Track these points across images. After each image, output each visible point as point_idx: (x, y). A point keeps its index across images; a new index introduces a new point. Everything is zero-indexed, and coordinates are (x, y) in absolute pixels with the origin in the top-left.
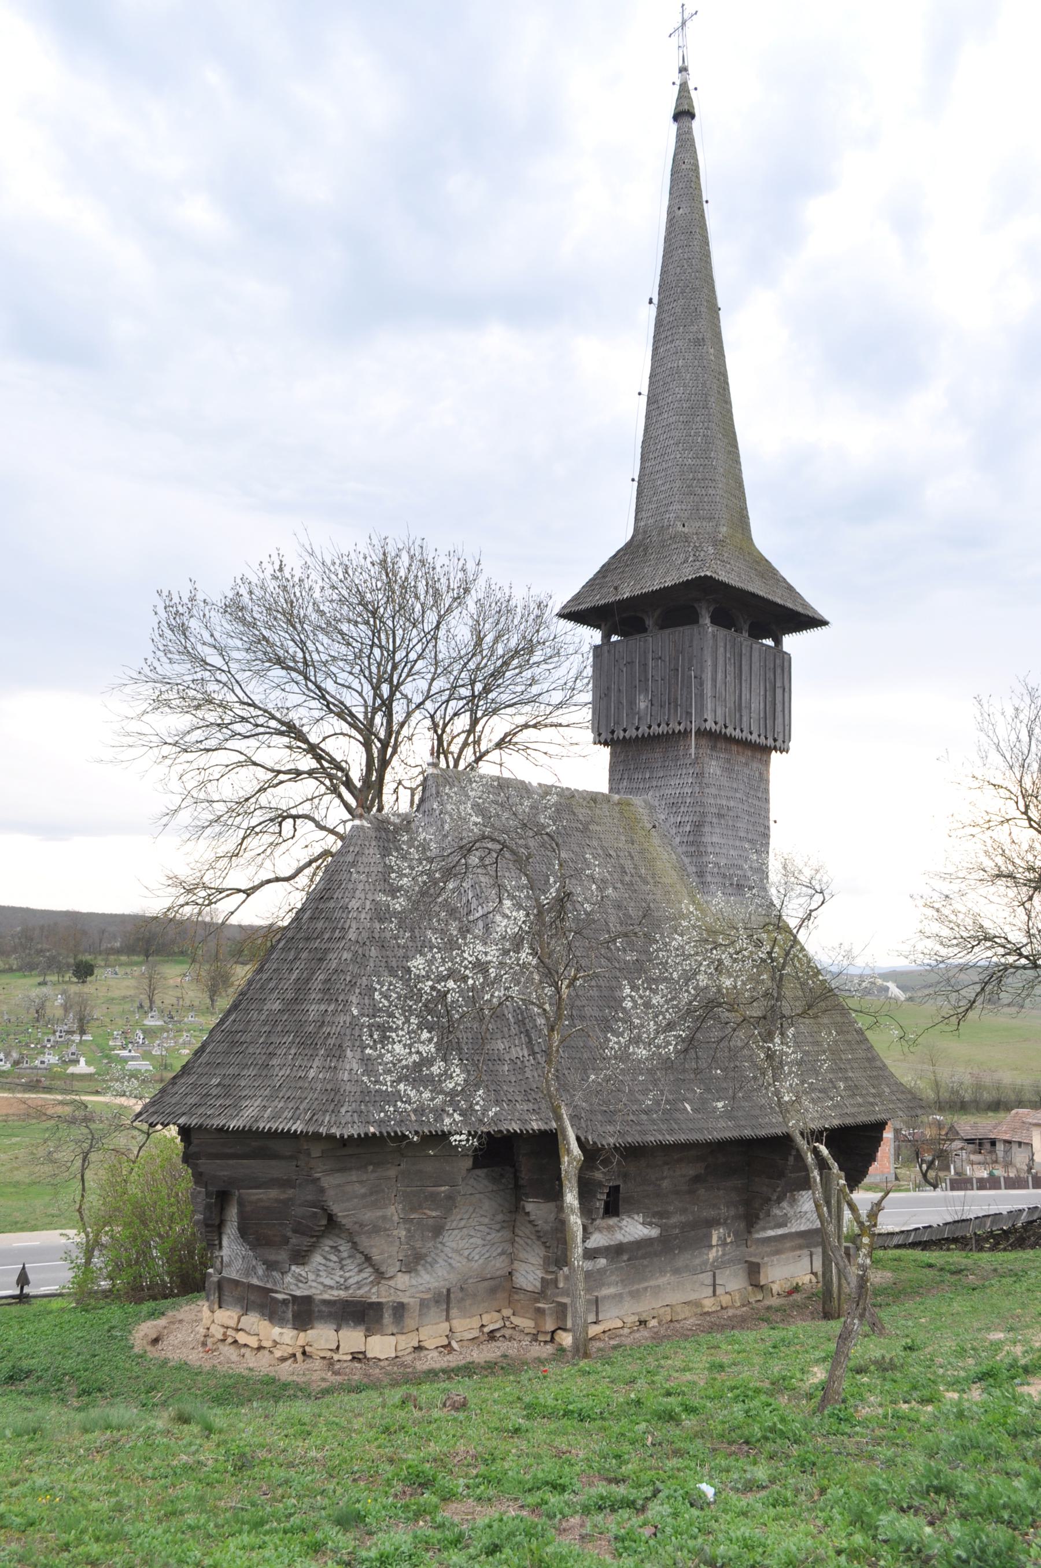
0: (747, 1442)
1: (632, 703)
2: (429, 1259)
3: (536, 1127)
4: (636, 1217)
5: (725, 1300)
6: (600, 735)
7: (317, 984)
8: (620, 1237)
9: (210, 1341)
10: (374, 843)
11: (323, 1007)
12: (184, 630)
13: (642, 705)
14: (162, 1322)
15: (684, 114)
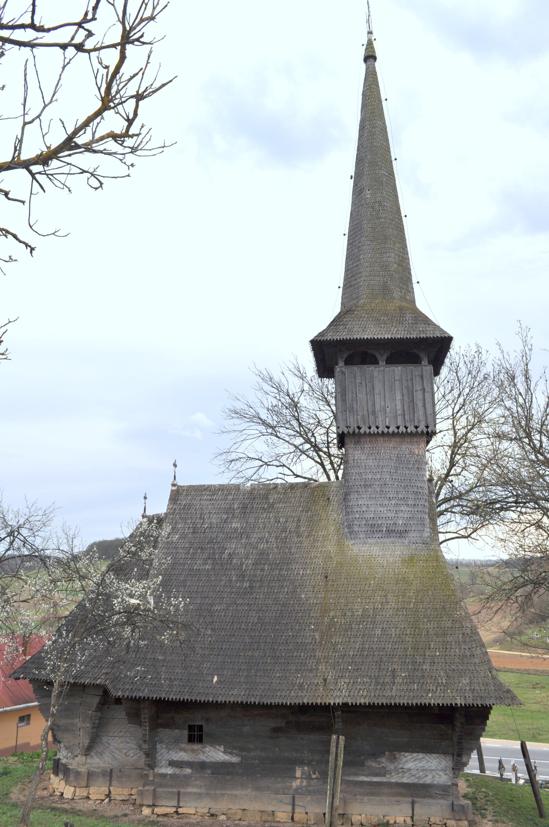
4: (218, 747)
8: (202, 757)
15: (370, 57)
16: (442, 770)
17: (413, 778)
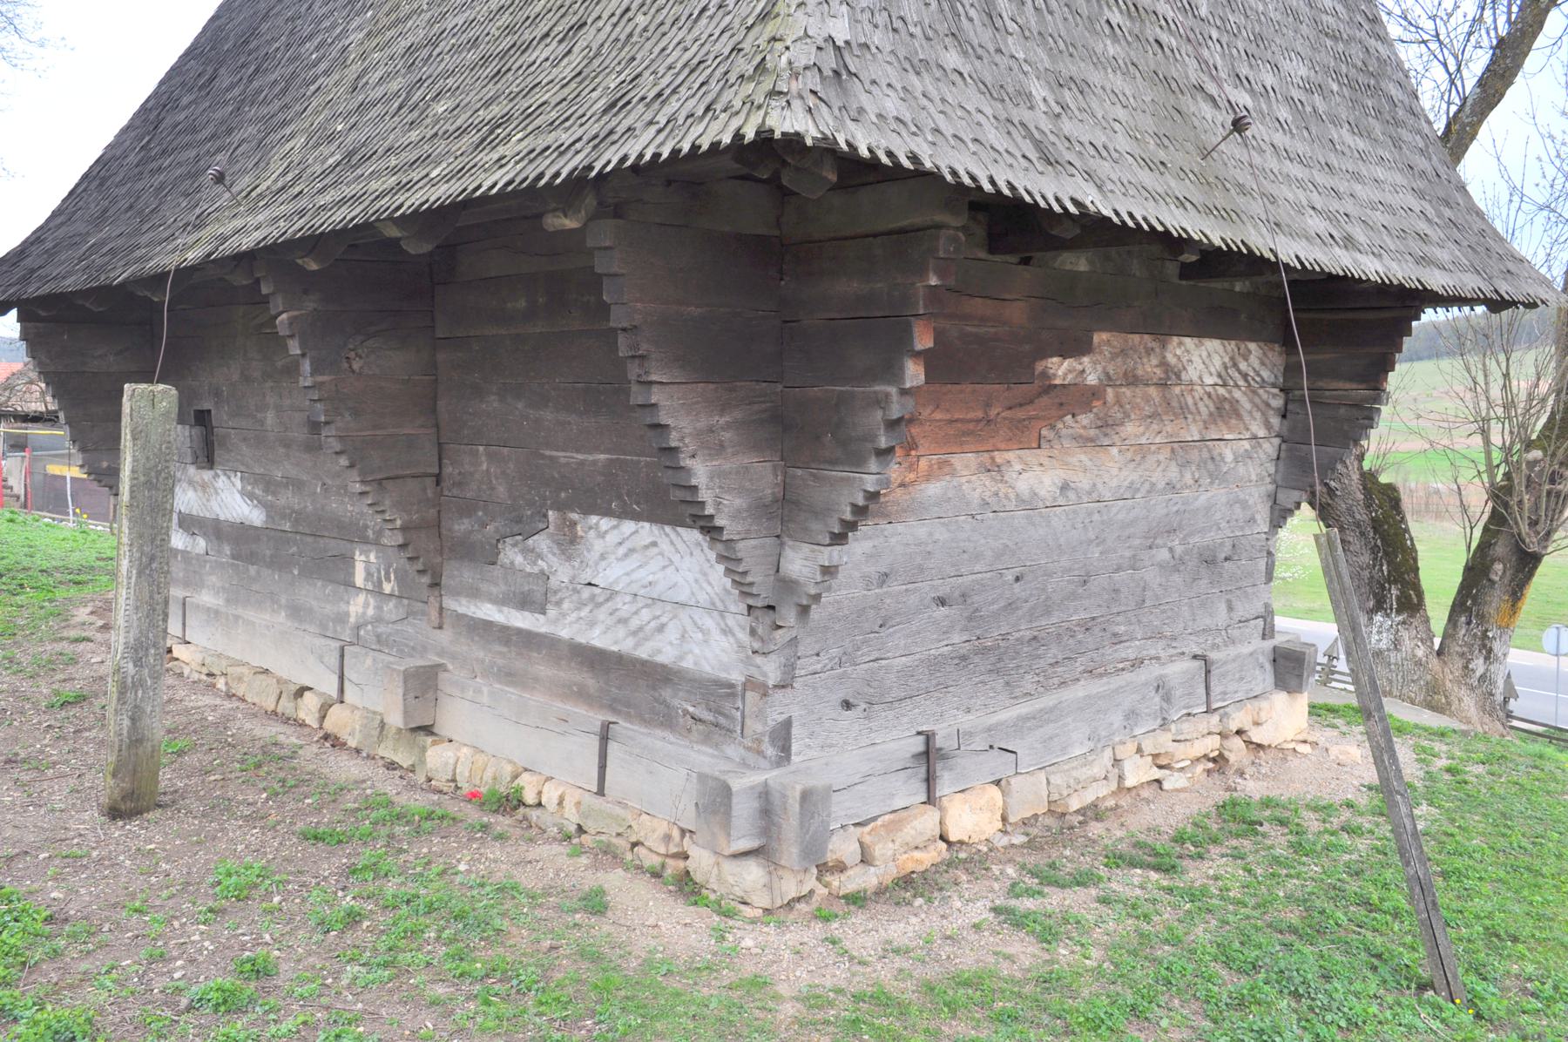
16: (711, 608)
17: (621, 632)
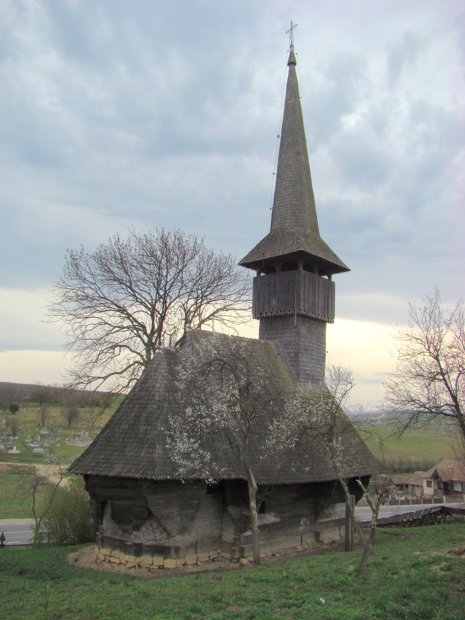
0: (332, 587)
1: (269, 302)
2: (189, 530)
3: (234, 477)
4: (271, 514)
5: (306, 546)
6: (255, 315)
7: (143, 418)
9: (98, 561)
10: (165, 360)
11: (146, 428)
12: (77, 266)
13: (274, 302)
14: (77, 553)
15: (292, 63)
